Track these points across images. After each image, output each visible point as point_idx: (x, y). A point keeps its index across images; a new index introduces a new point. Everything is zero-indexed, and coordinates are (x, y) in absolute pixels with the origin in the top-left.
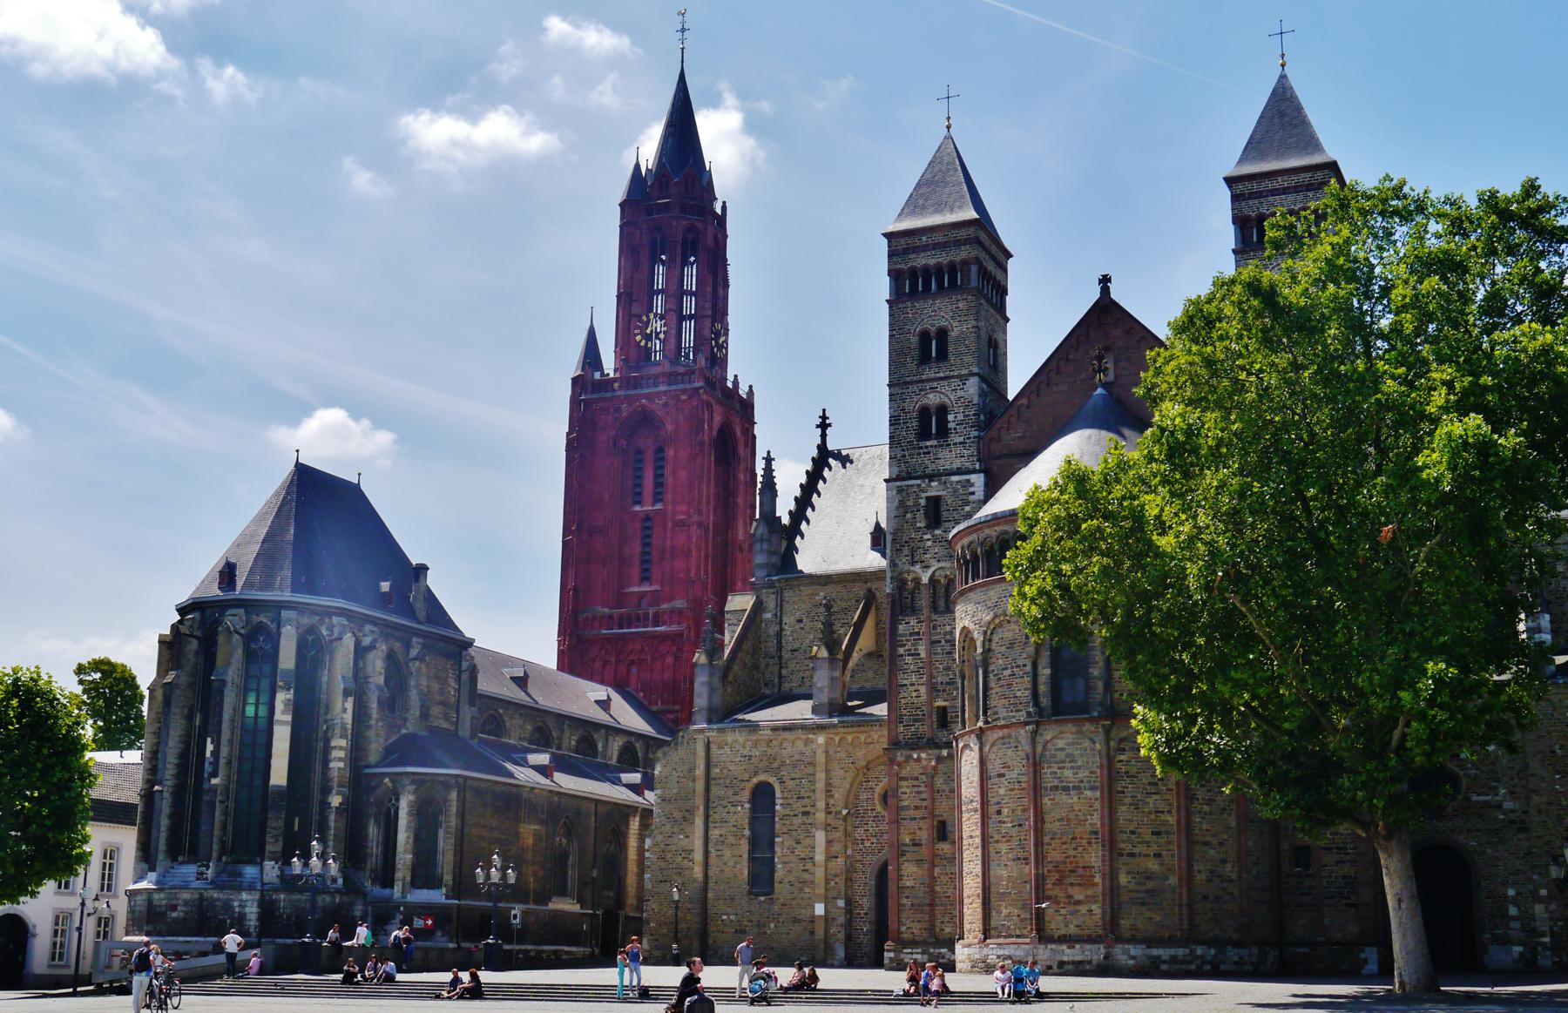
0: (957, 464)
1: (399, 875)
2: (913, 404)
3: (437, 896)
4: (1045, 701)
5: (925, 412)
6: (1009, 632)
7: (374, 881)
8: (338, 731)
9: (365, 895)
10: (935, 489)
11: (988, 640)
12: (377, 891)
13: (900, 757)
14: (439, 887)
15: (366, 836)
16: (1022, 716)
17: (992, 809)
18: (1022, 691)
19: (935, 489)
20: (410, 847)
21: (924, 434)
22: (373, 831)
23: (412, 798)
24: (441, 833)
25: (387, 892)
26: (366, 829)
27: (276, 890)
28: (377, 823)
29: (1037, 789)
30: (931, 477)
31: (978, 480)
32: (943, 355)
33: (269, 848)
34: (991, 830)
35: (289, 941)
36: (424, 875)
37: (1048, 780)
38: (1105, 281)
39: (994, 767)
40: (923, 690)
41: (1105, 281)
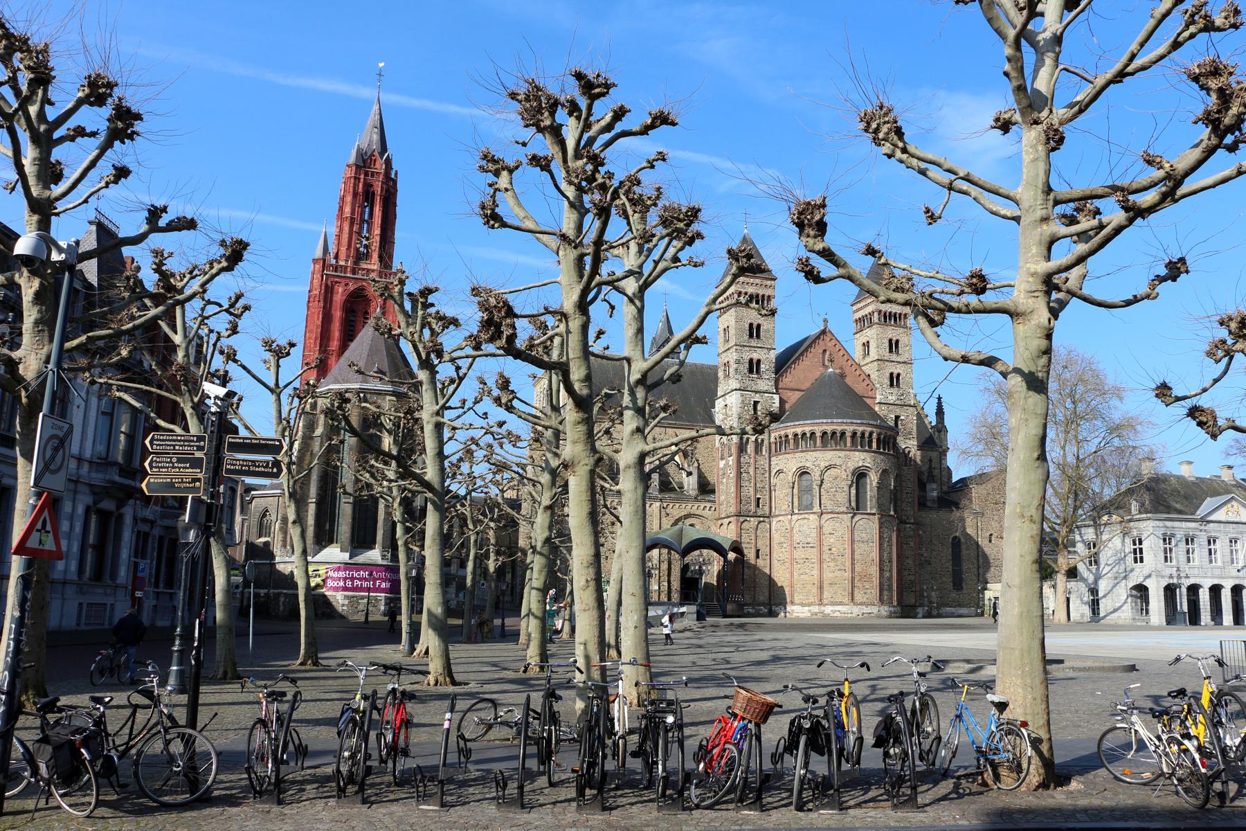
0: (766, 388)
2: (747, 356)
4: (854, 504)
5: (751, 361)
6: (832, 472)
10: (757, 397)
11: (822, 474)
13: (742, 519)
16: (844, 509)
17: (825, 548)
18: (842, 497)
19: (757, 397)
21: (751, 371)
29: (853, 541)
30: (756, 392)
31: (776, 397)
32: (758, 336)
34: (825, 556)
37: (856, 538)
38: (825, 321)
39: (828, 527)
40: (752, 490)
41: (825, 321)
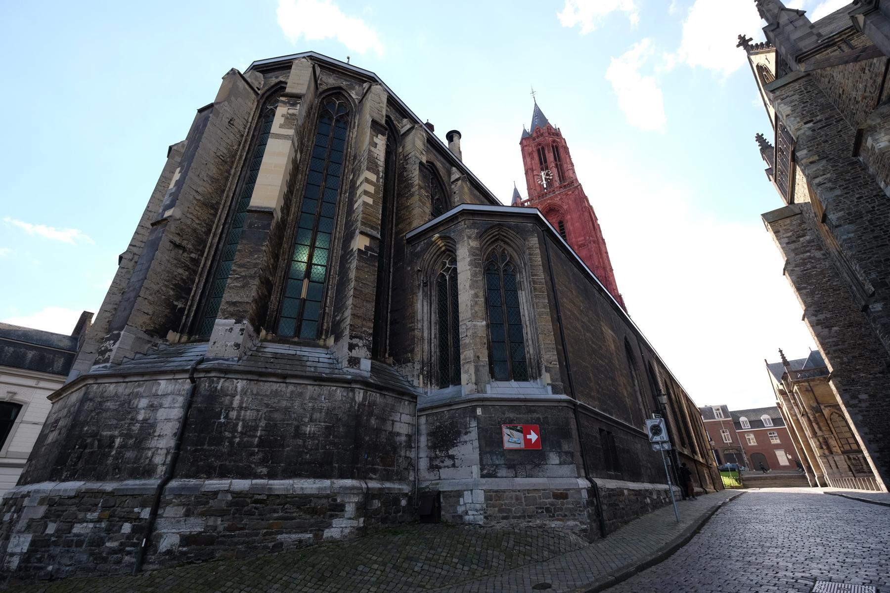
1: (467, 354)
3: (538, 389)
7: (428, 378)
8: (364, 166)
9: (414, 398)
12: (431, 393)
14: (536, 376)
15: (413, 316)
20: (481, 309)
22: (423, 310)
23: (474, 244)
24: (523, 297)
25: (451, 390)
26: (412, 304)
27: (226, 372)
28: (428, 296)
33: (228, 296)
35: (241, 484)
36: (508, 360)
